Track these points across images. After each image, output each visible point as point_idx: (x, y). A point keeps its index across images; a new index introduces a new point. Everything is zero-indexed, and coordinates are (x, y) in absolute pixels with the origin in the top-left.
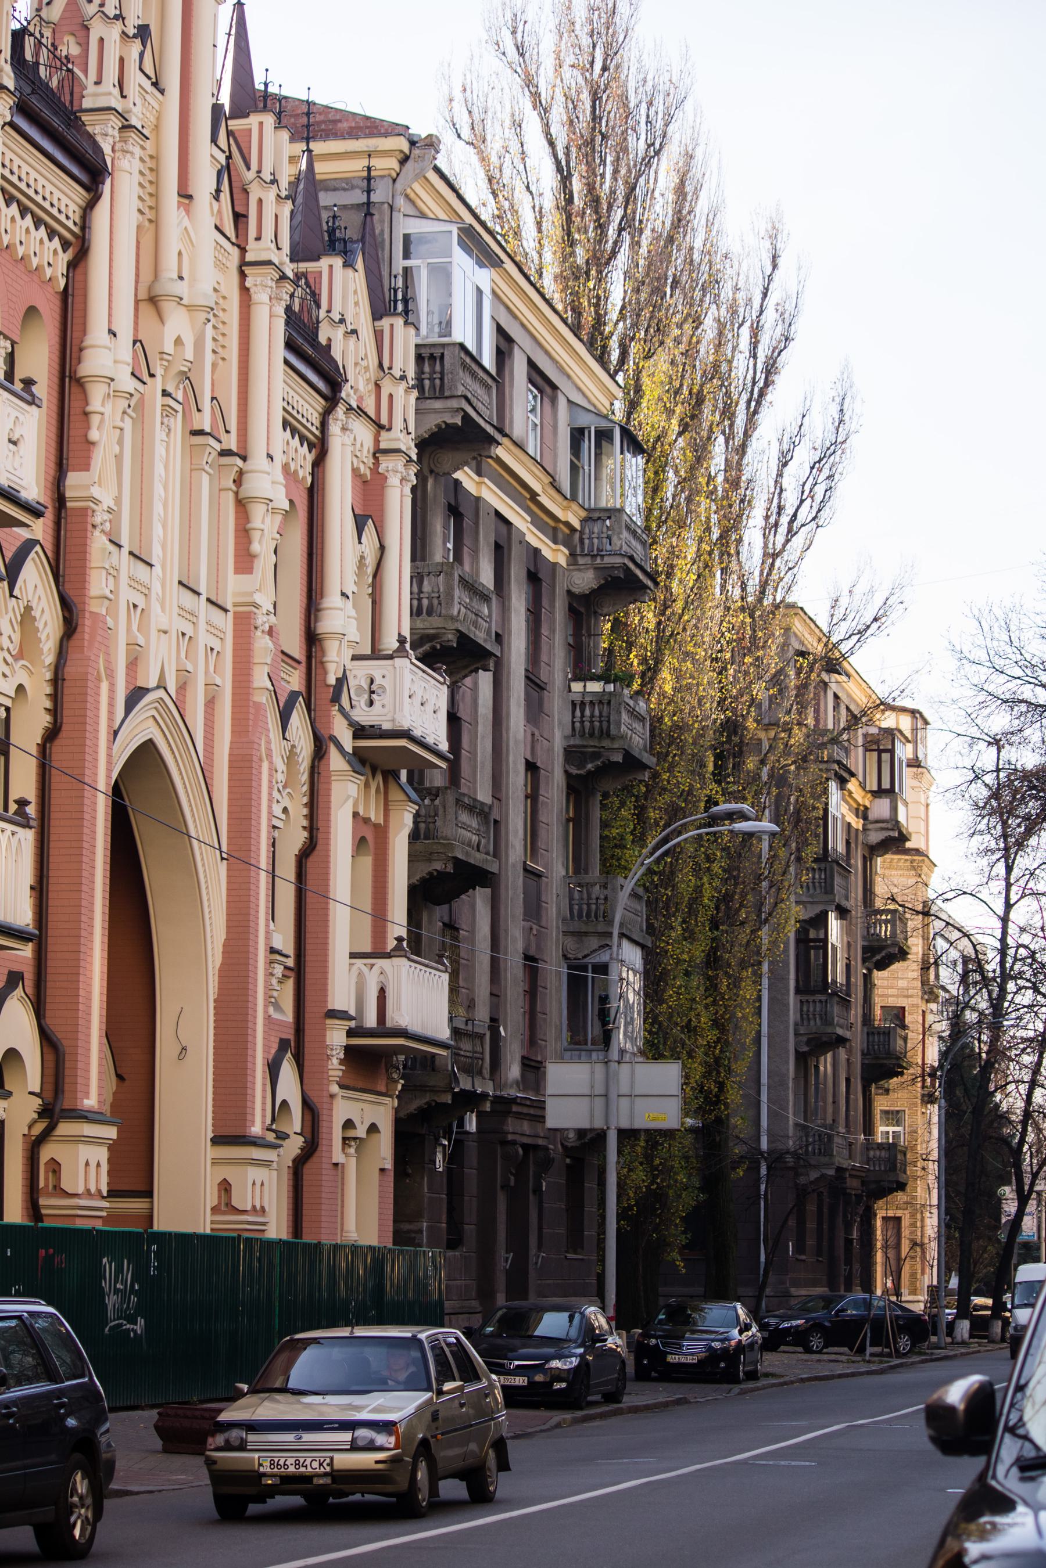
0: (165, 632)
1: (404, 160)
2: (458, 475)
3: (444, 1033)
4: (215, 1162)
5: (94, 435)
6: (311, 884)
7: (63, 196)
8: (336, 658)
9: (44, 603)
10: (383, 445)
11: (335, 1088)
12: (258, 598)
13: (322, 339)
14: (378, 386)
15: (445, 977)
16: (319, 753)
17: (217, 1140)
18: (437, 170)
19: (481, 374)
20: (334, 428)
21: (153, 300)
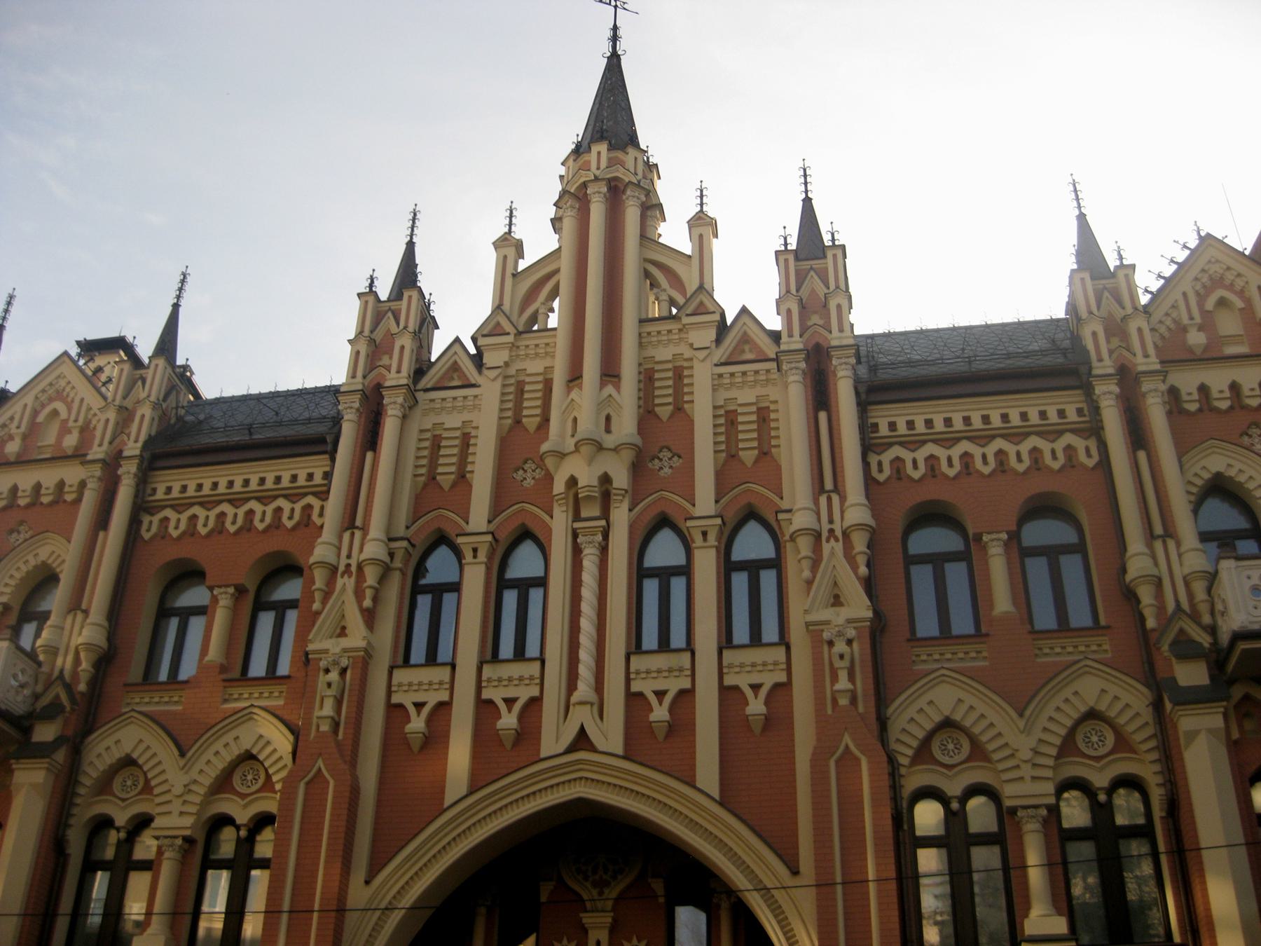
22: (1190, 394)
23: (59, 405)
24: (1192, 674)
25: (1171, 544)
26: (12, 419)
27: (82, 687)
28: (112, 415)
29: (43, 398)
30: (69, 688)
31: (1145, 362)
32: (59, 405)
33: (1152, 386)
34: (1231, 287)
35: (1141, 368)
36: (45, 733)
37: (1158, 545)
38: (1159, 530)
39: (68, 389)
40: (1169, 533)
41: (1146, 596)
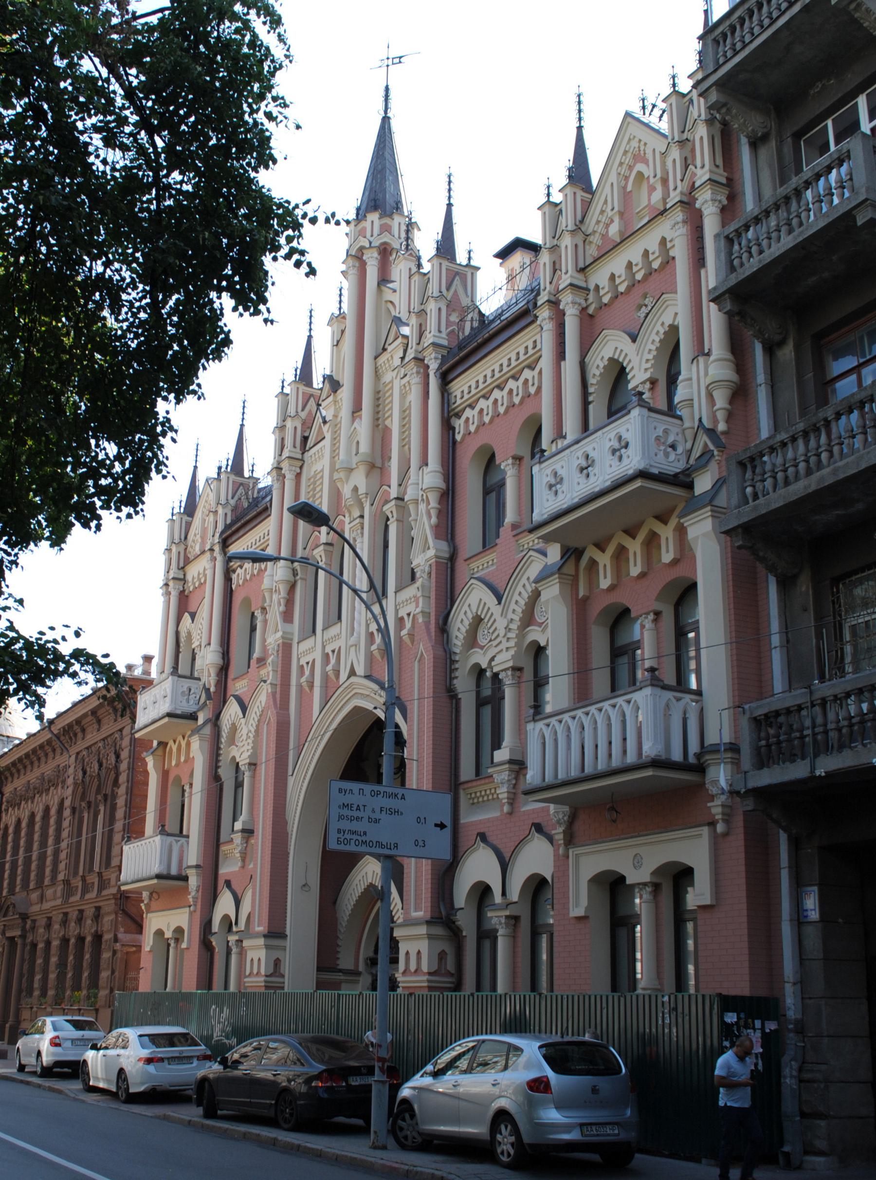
23: (640, 167)
26: (606, 202)
27: (722, 427)
28: (675, 154)
29: (624, 170)
30: (711, 432)
32: (640, 167)
36: (703, 484)
39: (642, 148)
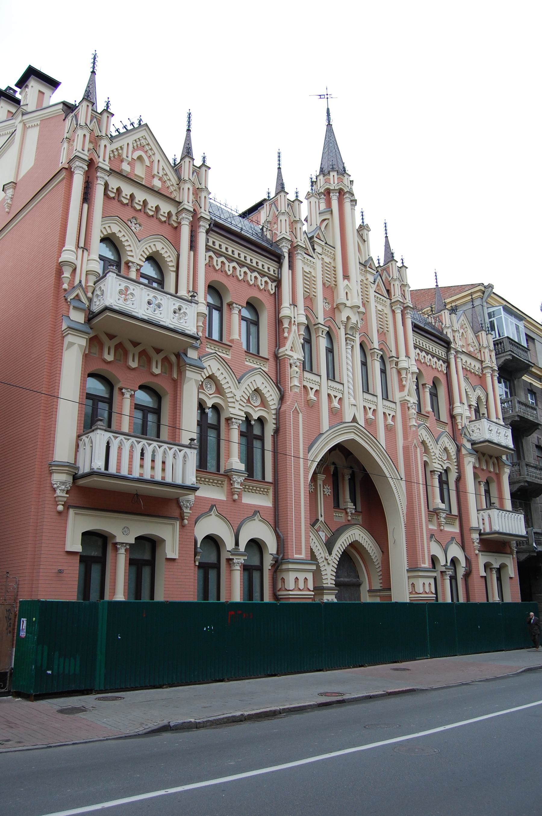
0: (355, 405)
1: (483, 293)
2: (523, 378)
3: (524, 533)
4: (409, 577)
5: (286, 334)
6: (461, 489)
7: (269, 266)
8: (461, 422)
9: (269, 388)
10: (483, 366)
11: (477, 552)
12: (407, 398)
13: (445, 333)
14: (480, 351)
15: (522, 516)
16: (459, 450)
17: (408, 571)
18: (494, 293)
19: (521, 347)
20: (452, 357)
21: (337, 307)
22: (113, 189)
24: (78, 317)
25: (86, 253)
31: (104, 163)
33: (102, 175)
34: (146, 152)
35: (100, 165)
37: (80, 251)
38: (82, 244)
40: (86, 248)
41: (67, 274)
